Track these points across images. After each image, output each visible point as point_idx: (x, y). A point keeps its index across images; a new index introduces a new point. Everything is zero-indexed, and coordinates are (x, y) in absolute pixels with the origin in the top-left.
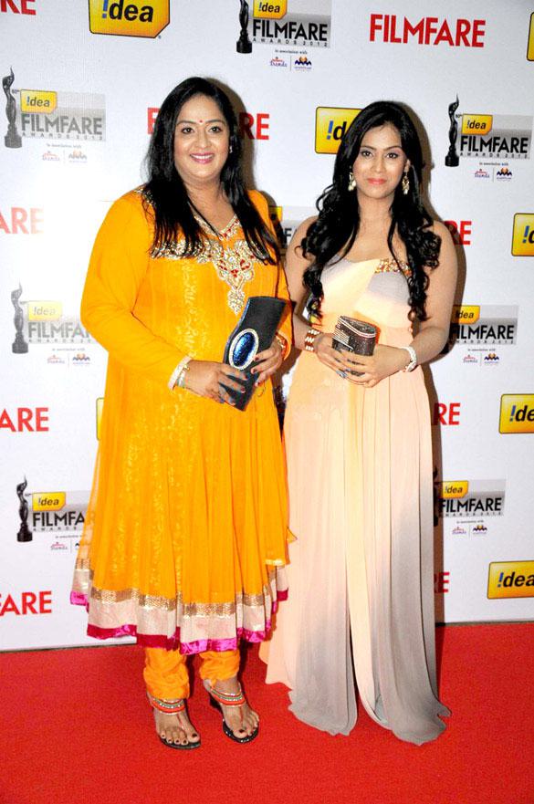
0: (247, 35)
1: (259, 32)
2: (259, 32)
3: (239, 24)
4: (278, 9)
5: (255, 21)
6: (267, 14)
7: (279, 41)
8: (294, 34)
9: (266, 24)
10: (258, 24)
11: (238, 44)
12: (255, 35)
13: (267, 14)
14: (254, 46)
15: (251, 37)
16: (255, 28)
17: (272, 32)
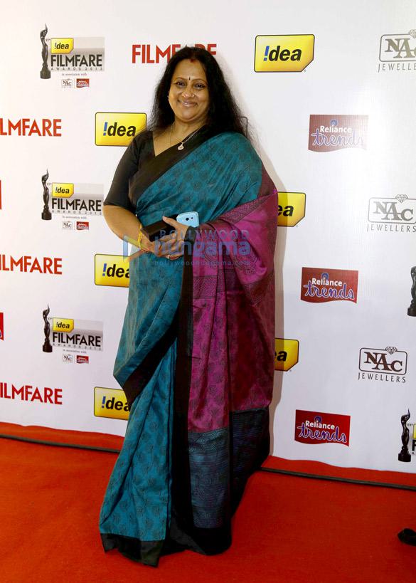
0: (48, 208)
1: (56, 206)
2: (56, 206)
3: (43, 201)
4: (68, 191)
5: (53, 199)
6: (61, 195)
7: (69, 212)
8: (79, 207)
9: (60, 201)
10: (55, 201)
11: (43, 214)
12: (53, 208)
13: (61, 195)
14: (53, 215)
15: (50, 209)
16: (53, 203)
17: (64, 206)
